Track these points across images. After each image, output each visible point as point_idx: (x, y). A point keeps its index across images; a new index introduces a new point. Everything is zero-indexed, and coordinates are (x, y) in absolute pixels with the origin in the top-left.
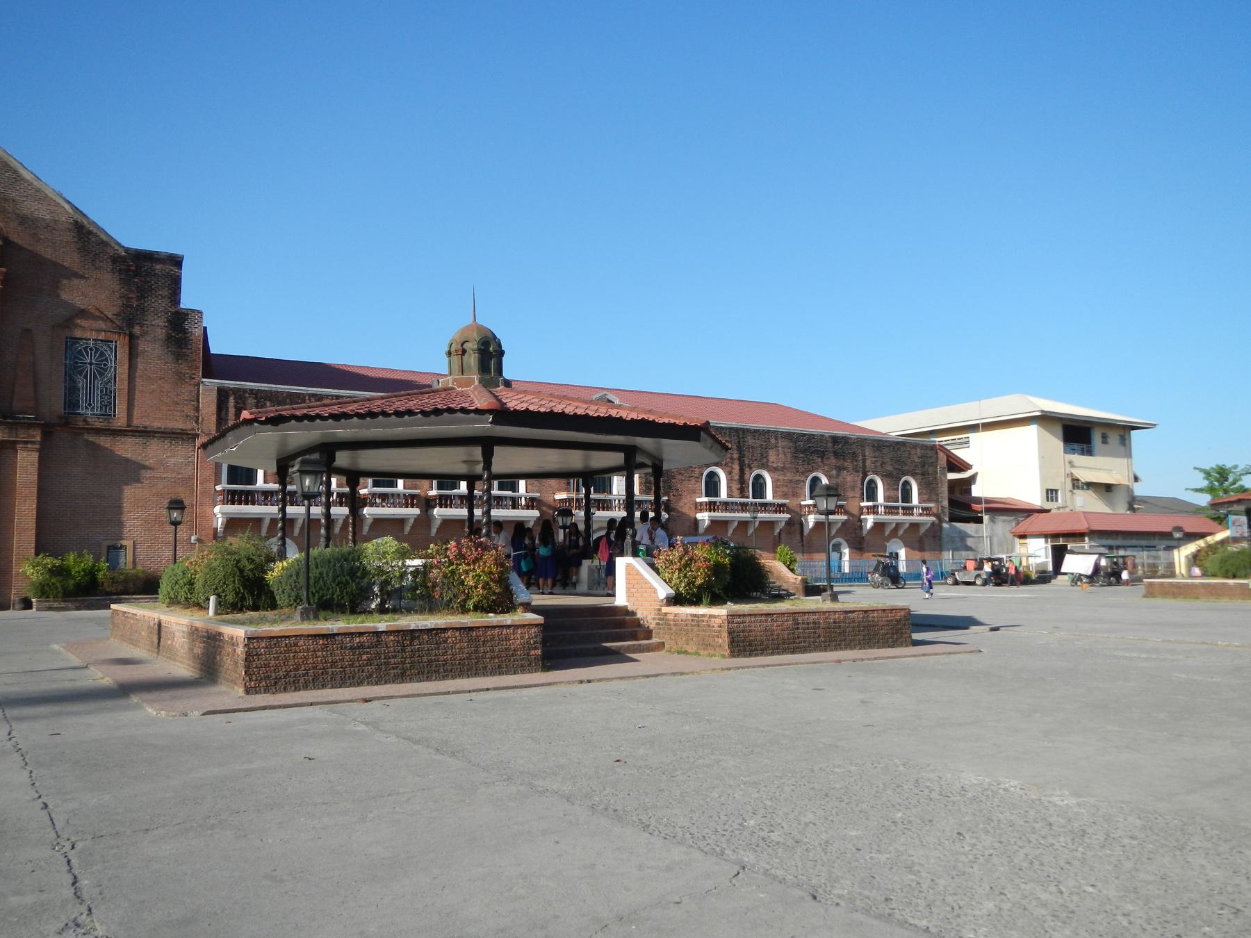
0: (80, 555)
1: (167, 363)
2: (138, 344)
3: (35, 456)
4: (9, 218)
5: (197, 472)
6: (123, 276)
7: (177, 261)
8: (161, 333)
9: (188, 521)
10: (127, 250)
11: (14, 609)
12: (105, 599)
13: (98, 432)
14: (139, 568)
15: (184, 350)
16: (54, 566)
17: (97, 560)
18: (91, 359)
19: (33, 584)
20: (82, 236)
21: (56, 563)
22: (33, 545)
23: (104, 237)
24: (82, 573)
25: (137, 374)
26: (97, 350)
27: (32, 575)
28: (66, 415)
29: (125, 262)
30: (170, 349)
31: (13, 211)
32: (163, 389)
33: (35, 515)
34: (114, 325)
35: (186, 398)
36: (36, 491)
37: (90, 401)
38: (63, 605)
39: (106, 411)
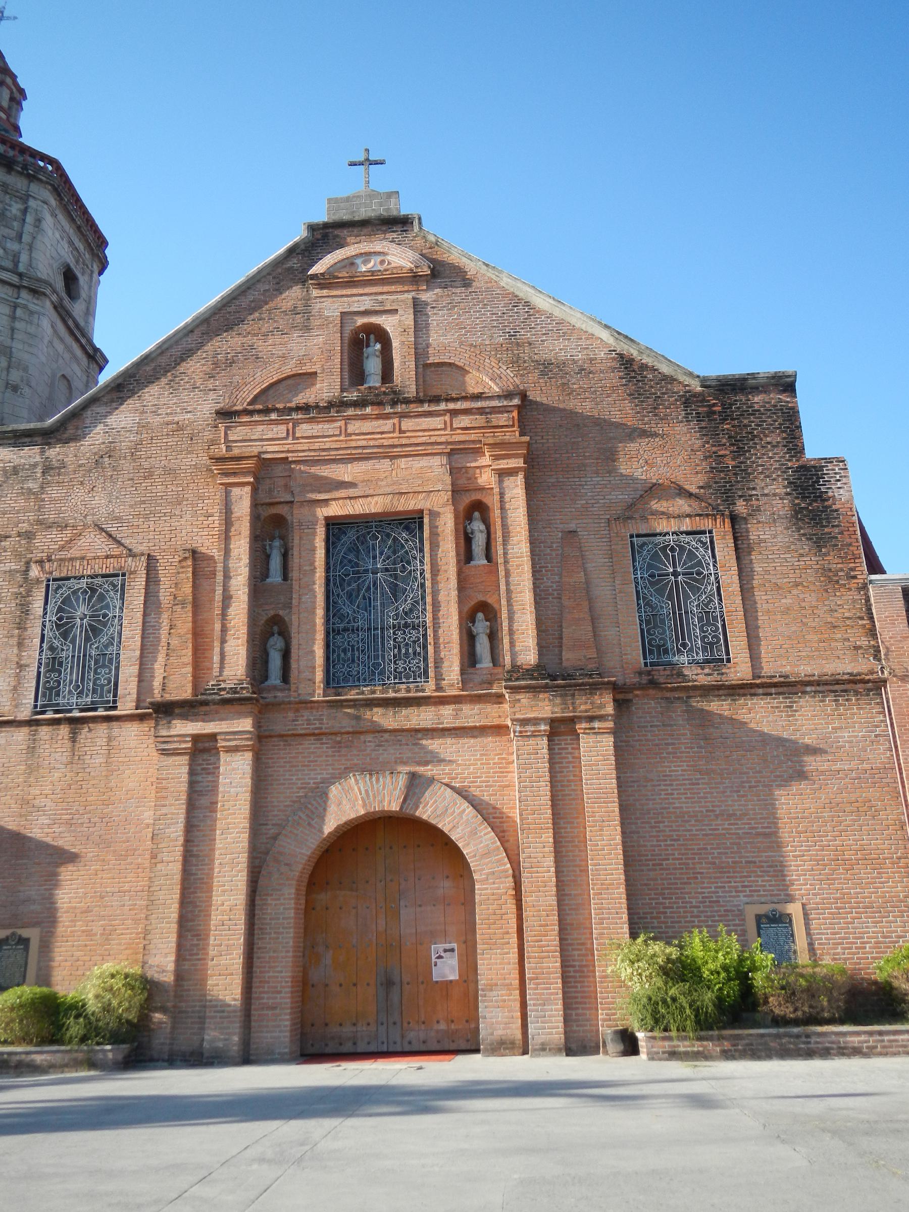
0: (714, 936)
1: (802, 555)
2: (748, 531)
3: (608, 742)
4: (525, 369)
5: (898, 755)
6: (703, 424)
8: (781, 506)
9: (899, 858)
10: (705, 382)
11: (606, 1053)
12: (778, 1036)
13: (708, 691)
14: (827, 961)
15: (826, 530)
16: (669, 960)
17: (745, 945)
18: (674, 566)
19: (636, 1000)
20: (633, 374)
21: (671, 954)
22: (625, 917)
23: (665, 369)
24: (723, 975)
25: (755, 583)
26: (682, 548)
27: (631, 979)
28: (649, 668)
29: (703, 400)
30: (802, 531)
31: (530, 358)
32: (803, 604)
33: (621, 857)
34: (703, 504)
35: (846, 615)
36: (617, 810)
37: (683, 639)
38: (697, 1047)
39: (712, 654)
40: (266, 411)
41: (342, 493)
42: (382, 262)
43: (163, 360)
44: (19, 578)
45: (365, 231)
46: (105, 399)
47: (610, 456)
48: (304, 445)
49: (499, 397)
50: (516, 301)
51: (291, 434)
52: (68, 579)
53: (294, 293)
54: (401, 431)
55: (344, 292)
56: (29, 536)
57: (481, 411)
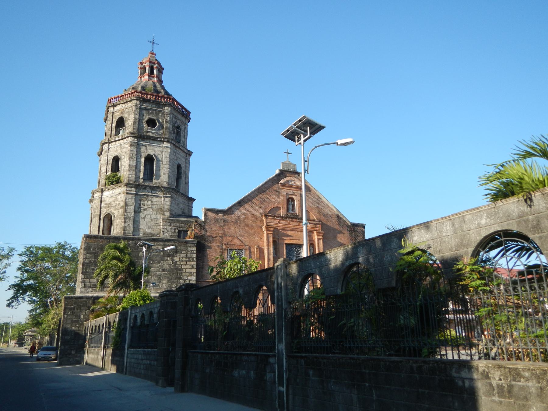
7: (363, 226)
10: (351, 223)
23: (344, 219)
40: (274, 216)
41: (288, 238)
42: (294, 183)
43: (249, 197)
44: (220, 247)
45: (291, 173)
46: (237, 205)
47: (335, 237)
48: (281, 225)
49: (318, 221)
50: (319, 198)
51: (279, 222)
52: (232, 249)
53: (276, 186)
54: (300, 226)
55: (286, 188)
56: (222, 237)
57: (314, 224)
